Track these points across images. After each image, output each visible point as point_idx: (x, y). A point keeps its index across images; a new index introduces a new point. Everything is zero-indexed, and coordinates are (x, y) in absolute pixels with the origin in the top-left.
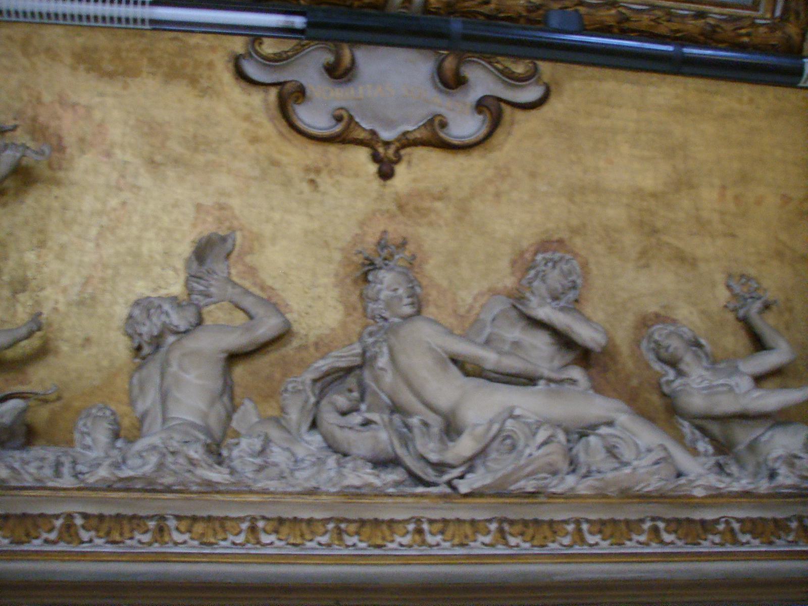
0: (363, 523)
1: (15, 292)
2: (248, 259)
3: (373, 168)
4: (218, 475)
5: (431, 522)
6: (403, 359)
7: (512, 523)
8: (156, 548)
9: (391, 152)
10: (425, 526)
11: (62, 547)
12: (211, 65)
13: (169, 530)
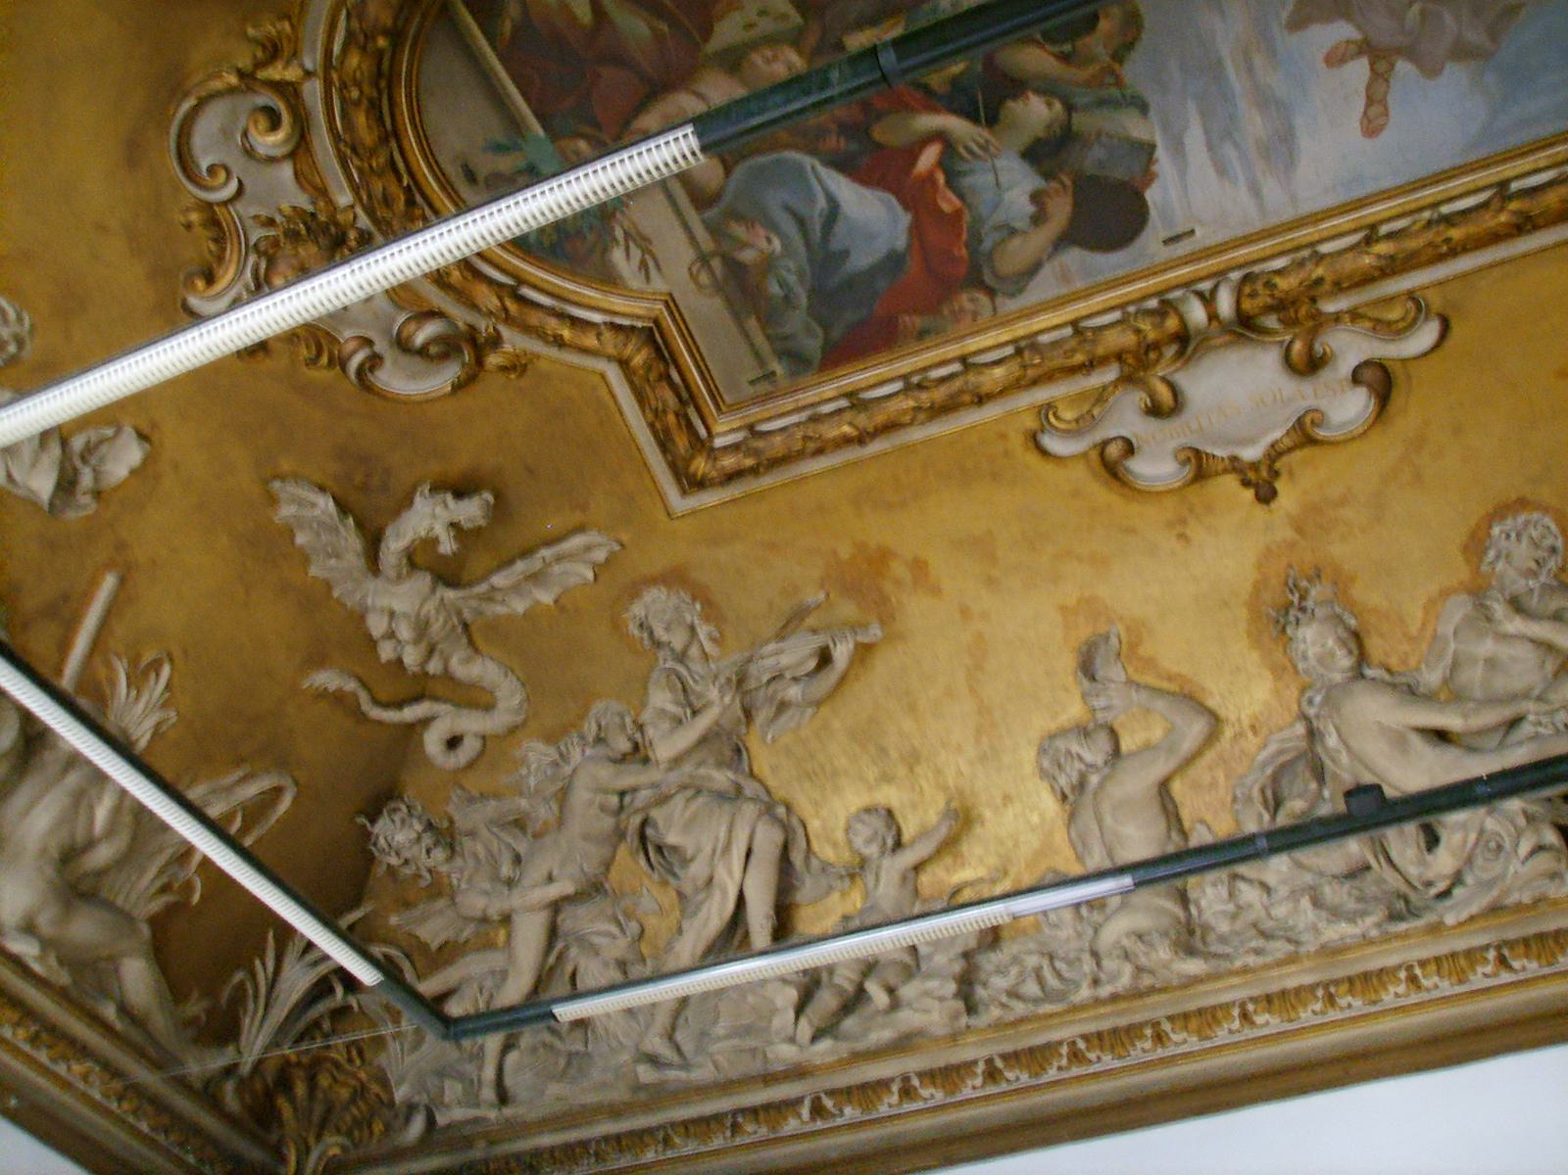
0: (1350, 980)
1: (911, 769)
2: (1143, 651)
3: (1249, 494)
4: (1194, 966)
5: (1423, 964)
6: (1353, 743)
7: (1511, 944)
8: (1160, 1053)
9: (1264, 473)
10: (1418, 971)
11: (1075, 1071)
12: (1007, 454)
13: (1167, 1034)
